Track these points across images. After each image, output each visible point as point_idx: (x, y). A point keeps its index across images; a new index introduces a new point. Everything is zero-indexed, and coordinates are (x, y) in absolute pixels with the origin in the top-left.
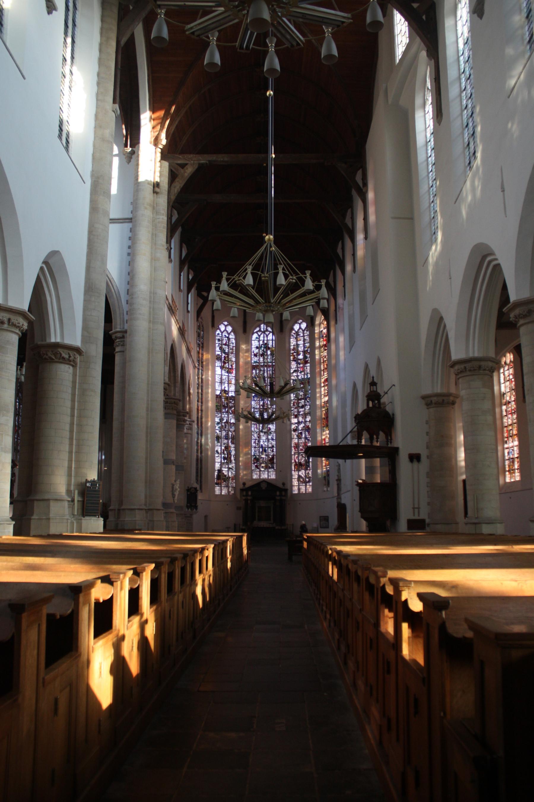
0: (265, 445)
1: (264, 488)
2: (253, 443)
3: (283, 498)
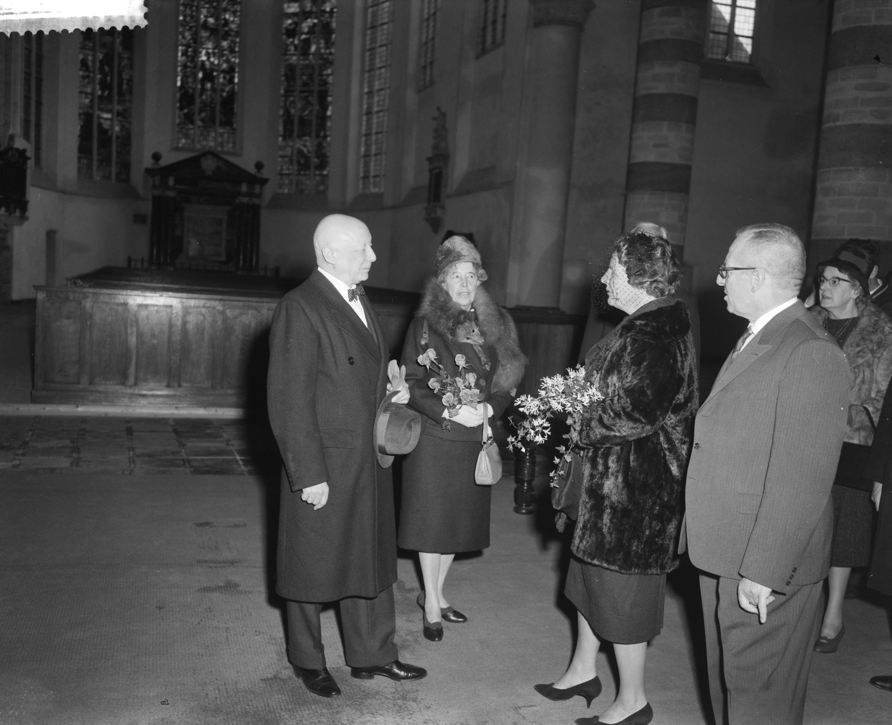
0: (212, 63)
1: (208, 173)
2: (180, 54)
3: (256, 201)
